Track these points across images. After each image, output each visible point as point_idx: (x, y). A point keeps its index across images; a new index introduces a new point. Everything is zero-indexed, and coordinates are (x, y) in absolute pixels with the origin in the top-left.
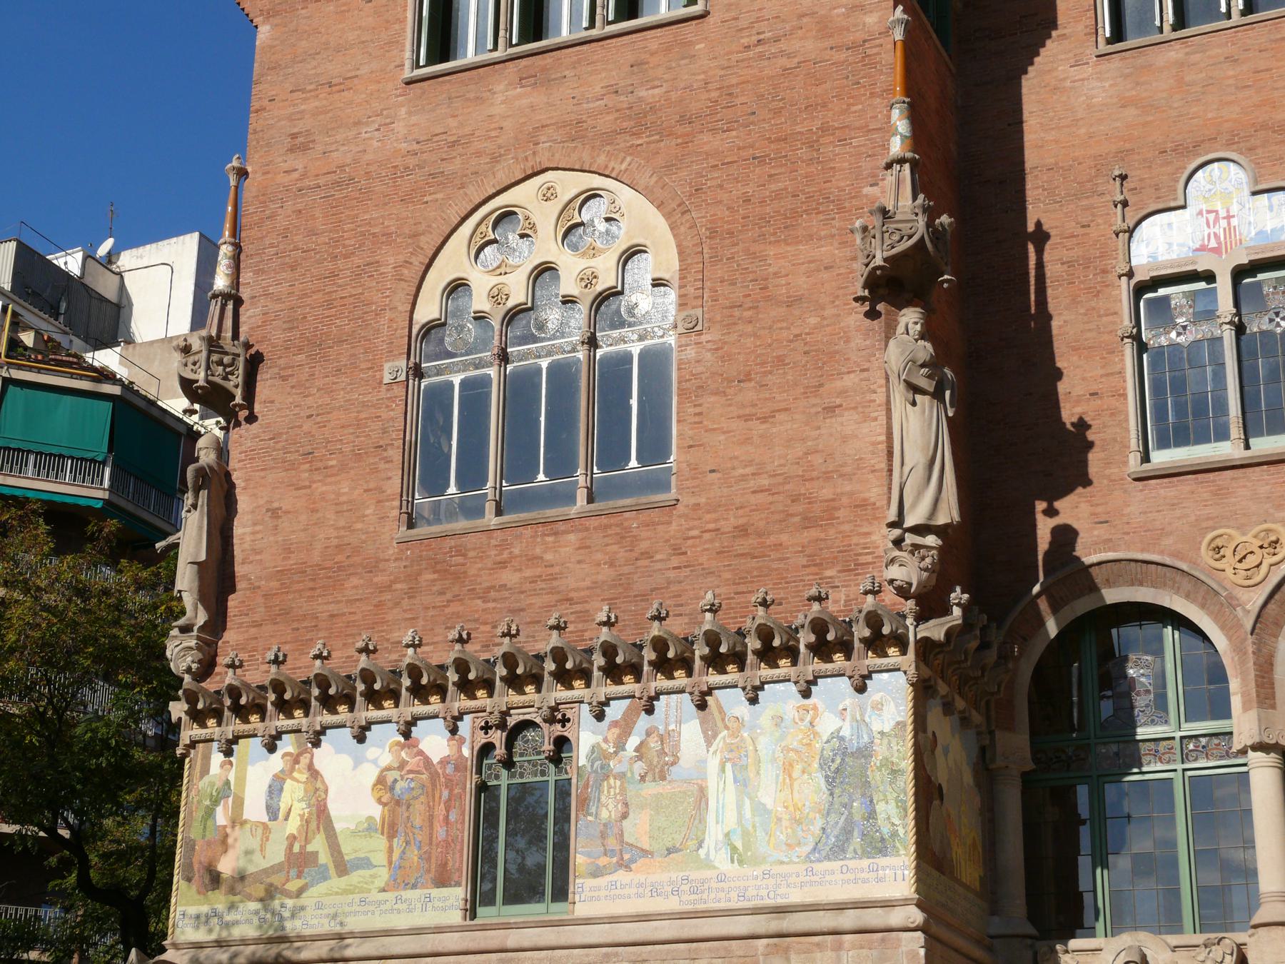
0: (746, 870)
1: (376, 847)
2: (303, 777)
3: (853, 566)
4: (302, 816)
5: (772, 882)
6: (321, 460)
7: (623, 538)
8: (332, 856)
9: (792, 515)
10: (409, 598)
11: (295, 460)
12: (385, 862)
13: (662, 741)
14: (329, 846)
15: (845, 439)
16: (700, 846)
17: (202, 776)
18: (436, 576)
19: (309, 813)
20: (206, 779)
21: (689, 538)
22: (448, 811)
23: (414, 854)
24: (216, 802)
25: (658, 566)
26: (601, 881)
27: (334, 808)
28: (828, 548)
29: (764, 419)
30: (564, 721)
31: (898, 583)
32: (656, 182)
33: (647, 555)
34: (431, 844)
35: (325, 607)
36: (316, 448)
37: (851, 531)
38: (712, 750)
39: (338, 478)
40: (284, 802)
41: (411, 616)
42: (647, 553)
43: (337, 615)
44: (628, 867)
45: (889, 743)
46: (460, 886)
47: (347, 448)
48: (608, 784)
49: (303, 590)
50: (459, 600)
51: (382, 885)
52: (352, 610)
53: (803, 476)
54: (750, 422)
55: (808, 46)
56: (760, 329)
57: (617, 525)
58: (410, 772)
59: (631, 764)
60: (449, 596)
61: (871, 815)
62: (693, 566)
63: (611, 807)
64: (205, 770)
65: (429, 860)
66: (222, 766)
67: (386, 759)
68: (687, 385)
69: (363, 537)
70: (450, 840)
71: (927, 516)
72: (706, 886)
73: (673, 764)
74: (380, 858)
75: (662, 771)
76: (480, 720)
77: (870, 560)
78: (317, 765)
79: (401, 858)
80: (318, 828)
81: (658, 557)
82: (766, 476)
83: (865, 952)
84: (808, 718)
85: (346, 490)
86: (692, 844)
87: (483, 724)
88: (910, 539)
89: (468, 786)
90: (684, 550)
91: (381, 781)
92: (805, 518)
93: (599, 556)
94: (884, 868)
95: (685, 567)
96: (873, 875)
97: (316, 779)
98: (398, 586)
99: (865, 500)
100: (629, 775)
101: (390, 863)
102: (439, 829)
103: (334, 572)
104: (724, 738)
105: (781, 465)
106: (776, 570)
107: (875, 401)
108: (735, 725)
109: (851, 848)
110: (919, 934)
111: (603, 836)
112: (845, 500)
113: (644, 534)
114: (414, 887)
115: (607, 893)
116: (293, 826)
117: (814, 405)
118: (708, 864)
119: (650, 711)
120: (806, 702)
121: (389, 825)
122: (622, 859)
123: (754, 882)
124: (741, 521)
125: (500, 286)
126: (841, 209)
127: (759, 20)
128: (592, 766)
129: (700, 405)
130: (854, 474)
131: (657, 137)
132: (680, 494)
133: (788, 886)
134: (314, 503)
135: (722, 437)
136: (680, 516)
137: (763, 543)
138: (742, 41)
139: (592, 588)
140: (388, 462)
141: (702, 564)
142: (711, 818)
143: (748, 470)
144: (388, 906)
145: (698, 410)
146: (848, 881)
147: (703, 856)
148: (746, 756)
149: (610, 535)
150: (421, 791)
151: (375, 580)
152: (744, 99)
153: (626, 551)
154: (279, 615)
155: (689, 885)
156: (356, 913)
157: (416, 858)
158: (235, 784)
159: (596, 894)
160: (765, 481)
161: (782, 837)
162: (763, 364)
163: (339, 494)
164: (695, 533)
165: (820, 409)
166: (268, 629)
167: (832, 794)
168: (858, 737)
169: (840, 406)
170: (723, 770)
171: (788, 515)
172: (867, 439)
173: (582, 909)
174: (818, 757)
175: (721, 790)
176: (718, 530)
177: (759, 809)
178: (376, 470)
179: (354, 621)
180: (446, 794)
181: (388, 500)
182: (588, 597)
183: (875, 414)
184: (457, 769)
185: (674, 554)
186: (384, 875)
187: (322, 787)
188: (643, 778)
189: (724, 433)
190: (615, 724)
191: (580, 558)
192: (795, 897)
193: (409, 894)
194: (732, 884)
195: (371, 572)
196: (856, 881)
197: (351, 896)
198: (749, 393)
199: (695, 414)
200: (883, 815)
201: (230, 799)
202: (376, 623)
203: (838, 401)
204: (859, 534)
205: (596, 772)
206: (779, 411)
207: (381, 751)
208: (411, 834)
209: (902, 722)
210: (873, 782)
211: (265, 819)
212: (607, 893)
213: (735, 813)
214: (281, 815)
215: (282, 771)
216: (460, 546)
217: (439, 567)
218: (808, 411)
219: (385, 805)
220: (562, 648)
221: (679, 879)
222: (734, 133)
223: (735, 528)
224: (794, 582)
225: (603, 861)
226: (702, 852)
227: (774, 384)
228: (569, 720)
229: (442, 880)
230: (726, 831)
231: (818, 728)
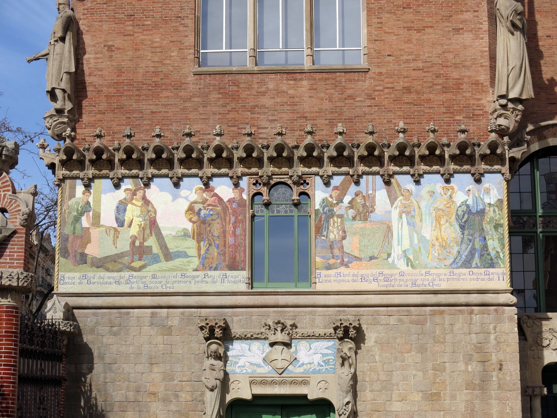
0: (417, 271)
1: (190, 246)
2: (140, 203)
3: (471, 116)
4: (140, 226)
5: (430, 278)
6: (140, 20)
7: (336, 86)
8: (161, 249)
9: (436, 84)
10: (203, 107)
11: (122, 18)
12: (196, 255)
13: (365, 199)
14: (159, 244)
15: (465, 47)
16: (389, 255)
17: (70, 198)
18: (220, 96)
19: (144, 224)
20: (73, 200)
21: (376, 91)
22: (235, 229)
23: (214, 251)
24: (82, 214)
25: (358, 104)
26: (332, 272)
27: (161, 222)
28: (457, 104)
29: (419, 31)
30: (305, 183)
31: (503, 127)
33: (351, 97)
34: (225, 246)
35: (148, 107)
36: (137, 13)
37: (470, 97)
39: (151, 32)
40: (128, 216)
41: (204, 117)
43: (156, 112)
44: (347, 266)
45: (494, 211)
46: (245, 270)
47: (157, 16)
48: (334, 220)
49: (132, 95)
50: (236, 111)
51: (195, 267)
52: (166, 110)
53: (442, 64)
54: (411, 31)
57: (332, 79)
58: (209, 205)
59: (347, 211)
60: (229, 107)
61: (485, 247)
62: (380, 106)
63: (335, 232)
64: (72, 195)
65: (224, 254)
66: (84, 194)
67: (194, 197)
68: (373, 6)
69: (171, 69)
70: (237, 244)
71: (519, 93)
72: (393, 278)
73: (371, 212)
74: (193, 252)
75: (365, 215)
76: (252, 180)
77: (481, 113)
78: (148, 198)
79: (206, 253)
80: (151, 233)
81: (358, 99)
82: (421, 62)
83: (486, 316)
84: (449, 193)
85: (158, 40)
86: (385, 256)
87: (254, 182)
88: (510, 105)
89: (247, 215)
91: (190, 209)
92: (444, 87)
93: (322, 95)
94: (492, 274)
95: (374, 106)
96: (488, 277)
97: (148, 205)
98: (196, 99)
99: (478, 81)
100: (345, 216)
101: (199, 255)
102: (230, 238)
103: (152, 87)
104: (401, 200)
105: (429, 57)
106: (428, 113)
107: (482, 28)
108: (407, 194)
109: (474, 263)
110: (514, 308)
111: (331, 247)
112: (466, 80)
113: (349, 86)
114: (216, 269)
115: (335, 278)
116: (134, 230)
117: (447, 26)
118: (393, 266)
119: (357, 183)
121: (197, 233)
122: (343, 261)
123: (421, 277)
124: (406, 85)
128: (323, 210)
129: (381, 18)
130: (471, 67)
132: (370, 66)
133: (440, 280)
134: (136, 45)
135: (395, 38)
136: (370, 78)
137: (419, 98)
139: (319, 112)
140: (185, 26)
141: (385, 106)
142: (395, 242)
143: (410, 57)
144: (199, 279)
145: (379, 21)
146: (474, 279)
147: (391, 262)
148: (414, 211)
149: (329, 84)
150: (216, 216)
151: (180, 94)
153: (339, 94)
154: (117, 108)
155: (383, 277)
156: (179, 282)
157: (216, 254)
158: (93, 204)
159: (329, 279)
160: (420, 65)
161: (435, 254)
163: (153, 42)
165: (451, 29)
166: (110, 115)
167: (463, 234)
168: (477, 205)
169: (462, 29)
170: (401, 217)
171: (434, 84)
172: (478, 49)
173: (319, 287)
174: (454, 215)
176: (394, 88)
177: (422, 239)
178: (176, 31)
179: (168, 117)
180: (233, 219)
181: (186, 49)
182: (316, 117)
183: (483, 36)
184: (239, 205)
185: (368, 99)
186: (196, 262)
187: (152, 210)
188: (354, 218)
189: (395, 35)
190: (336, 188)
191: (311, 95)
192: (444, 286)
193: (212, 273)
194: (408, 278)
195: (177, 89)
196: (477, 279)
197: (175, 273)
198: (409, 16)
199: (378, 23)
200: (492, 246)
201: (91, 213)
202: (182, 119)
203: (461, 26)
204: (474, 99)
205: (325, 213)
206: (427, 27)
207: (190, 192)
208: (212, 240)
209: (500, 199)
210: (485, 229)
211: (116, 225)
212: (335, 278)
213: (408, 241)
214: (126, 224)
215: (125, 199)
216: (235, 80)
217: (221, 91)
218: (444, 29)
219: (194, 222)
220: (313, 144)
221: (378, 273)
223: (403, 88)
224: (439, 120)
225: (332, 261)
226: (390, 260)
227: (424, 12)
228: (308, 184)
229: (233, 267)
230: (403, 249)
231: (454, 199)
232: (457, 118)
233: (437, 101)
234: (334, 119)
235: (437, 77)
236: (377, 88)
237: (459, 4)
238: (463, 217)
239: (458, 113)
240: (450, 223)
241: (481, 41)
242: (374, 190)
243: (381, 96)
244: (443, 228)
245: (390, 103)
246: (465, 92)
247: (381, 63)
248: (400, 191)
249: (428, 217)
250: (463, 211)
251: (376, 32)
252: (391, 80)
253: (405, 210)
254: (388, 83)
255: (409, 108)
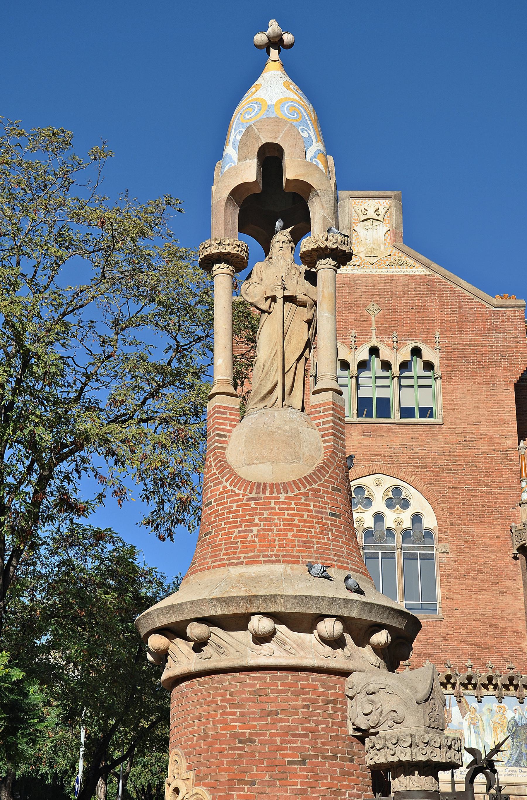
21: (449, 634)
25: (436, 643)
29: (476, 592)
32: (426, 489)
33: (431, 638)
38: (465, 718)
42: (432, 638)
55: (485, 447)
56: (471, 556)
62: (451, 645)
68: (444, 573)
84: (502, 711)
90: (447, 639)
106: (484, 652)
109: (522, 763)
120: (500, 704)
125: (360, 518)
126: (502, 515)
127: (464, 431)
129: (450, 582)
130: (513, 619)
131: (425, 470)
138: (458, 439)
145: (449, 584)
148: (478, 723)
152: (459, 462)
160: (478, 617)
162: (474, 570)
164: (452, 633)
167: (513, 741)
170: (469, 727)
171: (488, 631)
175: (469, 735)
183: (520, 598)
189: (460, 595)
198: (469, 582)
204: (516, 643)
206: (482, 590)
222: (457, 475)
227: (479, 579)
232: (505, 656)
233: (490, 643)
234: (421, 654)
235: (490, 626)
236: (449, 633)
237: (503, 574)
238: (512, 729)
239: (506, 653)
240: (504, 733)
241: (519, 601)
242: (450, 707)
243: (452, 638)
244: (499, 736)
245: (459, 644)
246: (510, 637)
247: (451, 614)
248: (468, 708)
249: (488, 728)
250: (512, 725)
251: (447, 592)
252: (459, 627)
253: (472, 722)
254: (457, 629)
255: (472, 648)
